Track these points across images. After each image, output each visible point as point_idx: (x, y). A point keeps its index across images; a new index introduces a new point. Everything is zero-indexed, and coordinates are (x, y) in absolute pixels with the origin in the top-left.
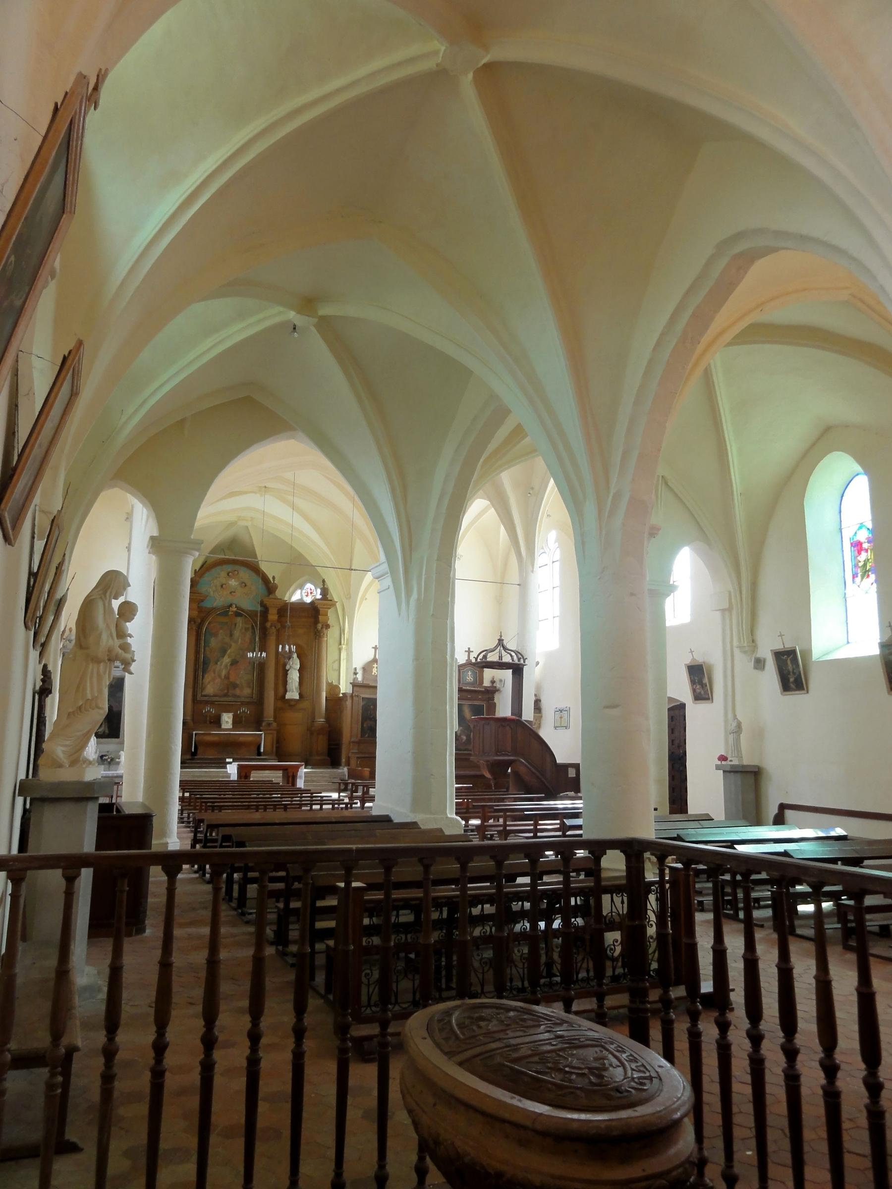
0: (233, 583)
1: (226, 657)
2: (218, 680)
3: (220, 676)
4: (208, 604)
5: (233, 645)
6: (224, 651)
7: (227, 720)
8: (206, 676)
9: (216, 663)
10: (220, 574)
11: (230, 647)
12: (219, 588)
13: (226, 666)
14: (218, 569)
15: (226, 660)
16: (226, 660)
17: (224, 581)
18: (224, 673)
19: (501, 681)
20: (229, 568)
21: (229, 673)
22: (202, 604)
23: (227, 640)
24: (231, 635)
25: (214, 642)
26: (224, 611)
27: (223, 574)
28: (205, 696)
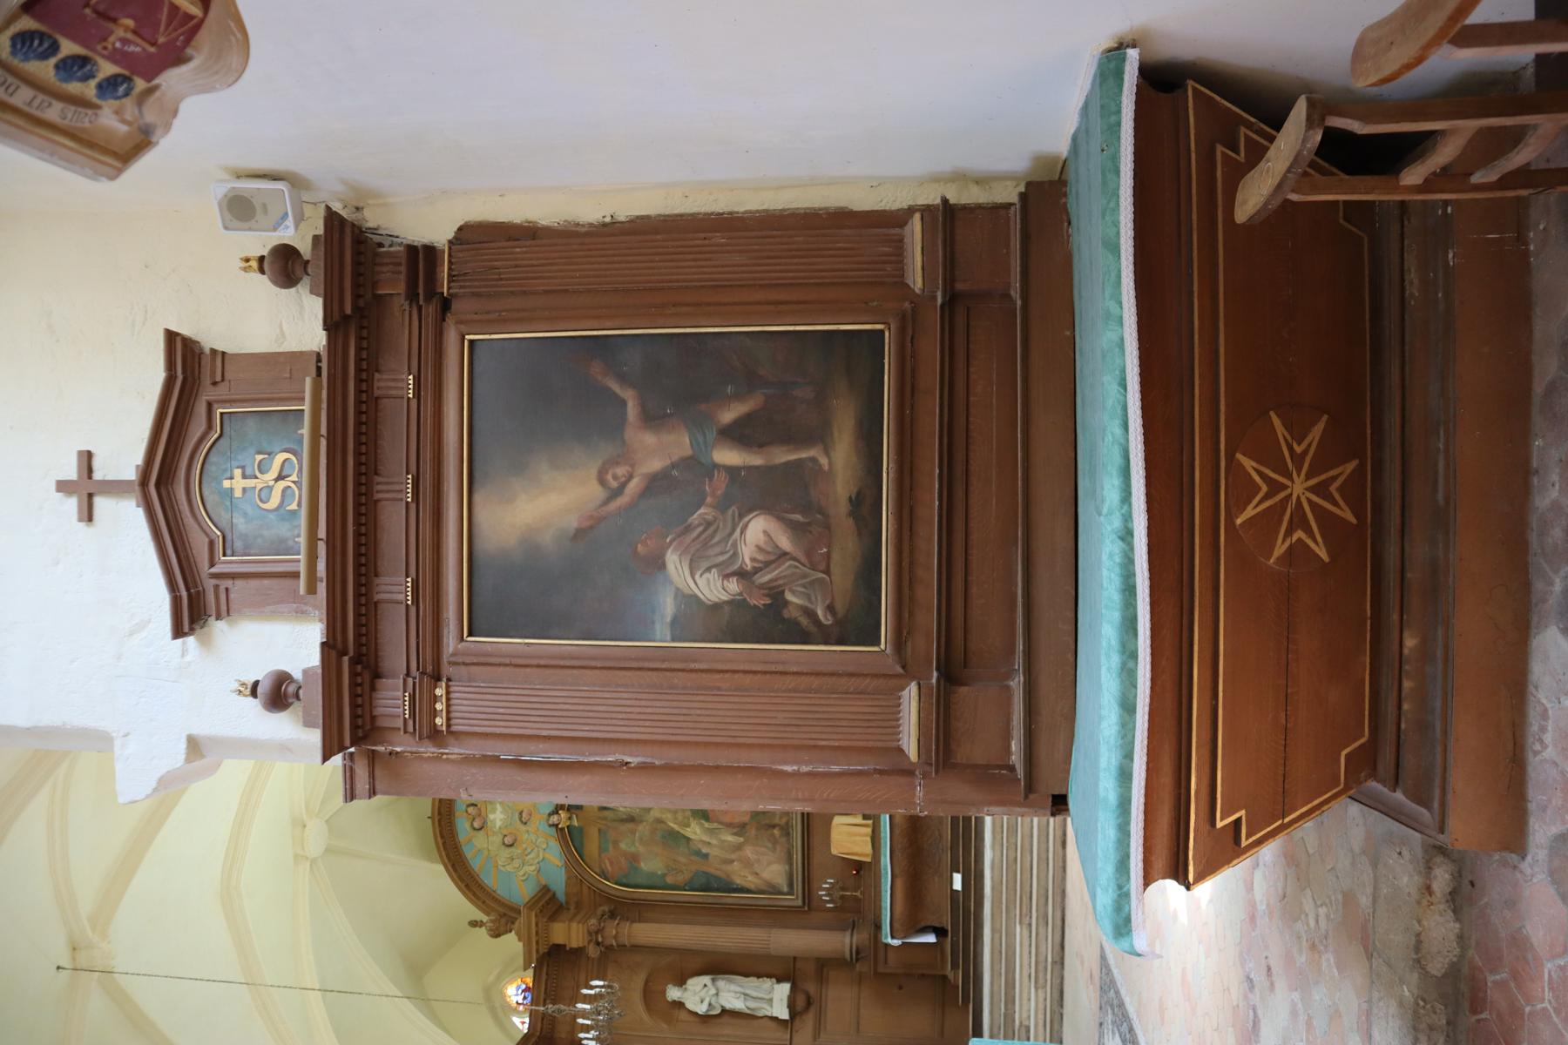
0: (497, 817)
1: (688, 832)
2: (749, 851)
3: (739, 847)
4: (558, 880)
5: (655, 814)
6: (674, 839)
7: (849, 837)
8: (738, 881)
9: (706, 856)
10: (476, 847)
11: (659, 821)
12: (516, 851)
13: (711, 831)
14: (468, 852)
15: (695, 831)
16: (695, 831)
17: (498, 839)
18: (730, 838)
19: (239, 209)
20: (463, 826)
21: (729, 825)
22: (561, 896)
23: (643, 829)
24: (631, 819)
25: (653, 864)
26: (571, 838)
27: (480, 840)
28: (791, 885)
